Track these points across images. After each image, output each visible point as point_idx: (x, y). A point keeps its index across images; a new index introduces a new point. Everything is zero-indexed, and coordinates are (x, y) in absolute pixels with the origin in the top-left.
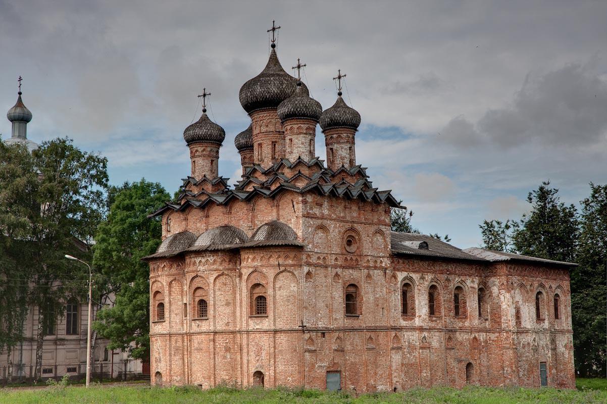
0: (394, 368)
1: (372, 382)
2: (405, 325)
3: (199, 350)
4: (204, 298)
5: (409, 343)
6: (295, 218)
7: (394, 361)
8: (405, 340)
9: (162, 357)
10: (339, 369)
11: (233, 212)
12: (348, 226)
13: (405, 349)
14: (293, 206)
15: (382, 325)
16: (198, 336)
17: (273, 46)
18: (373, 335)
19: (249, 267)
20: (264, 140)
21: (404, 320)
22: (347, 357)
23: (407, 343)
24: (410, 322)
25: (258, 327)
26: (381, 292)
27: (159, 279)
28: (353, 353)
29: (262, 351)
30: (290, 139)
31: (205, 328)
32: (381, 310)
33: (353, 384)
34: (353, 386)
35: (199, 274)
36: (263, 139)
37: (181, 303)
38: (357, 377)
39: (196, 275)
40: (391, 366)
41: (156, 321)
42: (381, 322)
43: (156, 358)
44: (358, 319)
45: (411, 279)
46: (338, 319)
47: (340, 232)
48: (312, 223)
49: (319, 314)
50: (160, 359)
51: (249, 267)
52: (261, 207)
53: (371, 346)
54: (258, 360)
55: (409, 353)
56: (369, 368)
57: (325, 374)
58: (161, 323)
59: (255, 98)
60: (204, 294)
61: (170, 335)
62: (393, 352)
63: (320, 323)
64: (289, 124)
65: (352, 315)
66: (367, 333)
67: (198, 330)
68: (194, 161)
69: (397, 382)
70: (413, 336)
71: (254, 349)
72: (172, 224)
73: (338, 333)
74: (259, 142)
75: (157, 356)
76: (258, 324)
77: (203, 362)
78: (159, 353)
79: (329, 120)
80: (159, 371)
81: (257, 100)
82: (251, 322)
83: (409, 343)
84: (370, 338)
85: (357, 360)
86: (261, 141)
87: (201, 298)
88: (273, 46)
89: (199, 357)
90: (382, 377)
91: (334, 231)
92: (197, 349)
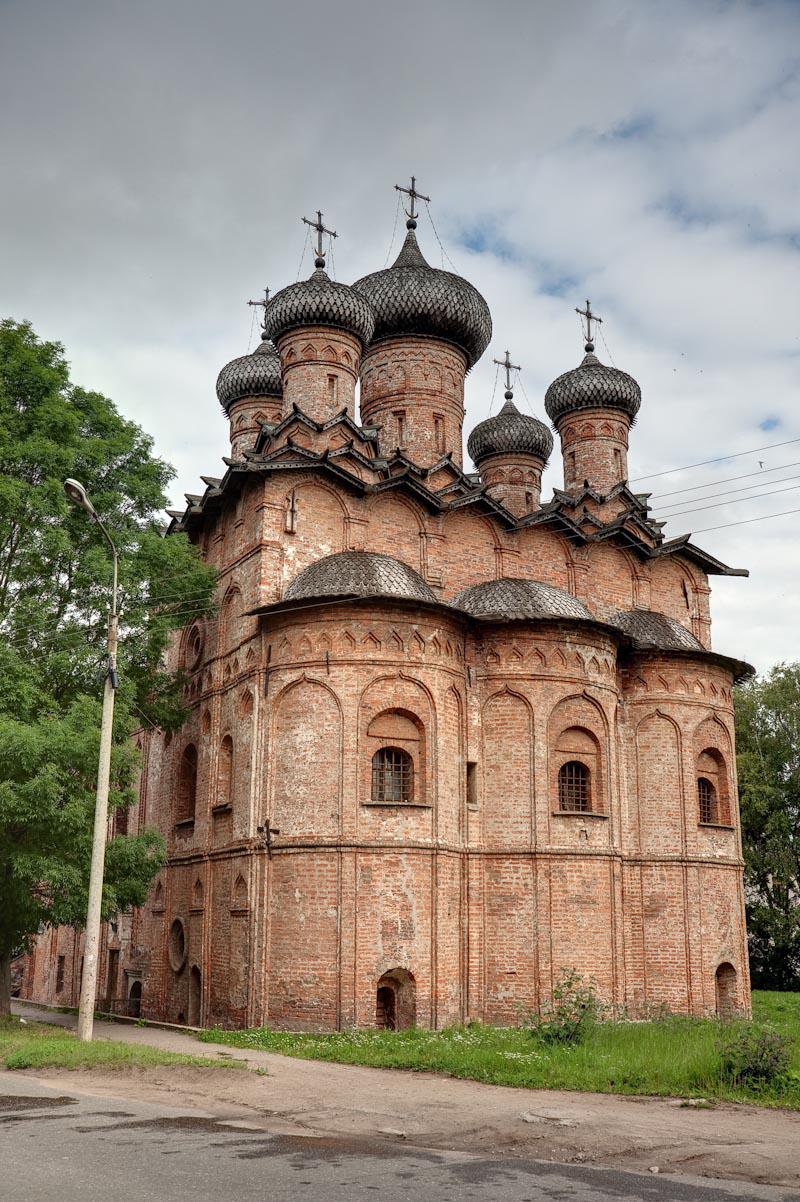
3: (584, 902)
4: (589, 761)
6: (690, 621)
9: (416, 920)
11: (524, 554)
14: (685, 595)
16: (583, 864)
17: (411, 225)
19: (700, 705)
20: (449, 411)
25: (720, 853)
27: (420, 674)
29: (731, 913)
30: (615, 449)
31: (600, 843)
35: (591, 691)
36: (448, 408)
37: (458, 759)
39: (580, 691)
41: (368, 800)
43: (385, 923)
50: (408, 932)
51: (700, 705)
52: (604, 569)
54: (724, 936)
58: (416, 811)
59: (464, 316)
60: (586, 749)
61: (435, 851)
64: (618, 418)
67: (581, 845)
68: (332, 378)
71: (716, 907)
72: (301, 516)
74: (436, 411)
75: (395, 916)
76: (721, 846)
77: (597, 937)
78: (406, 908)
79: (541, 437)
80: (403, 964)
81: (467, 321)
82: (705, 839)
86: (444, 413)
87: (574, 757)
88: (411, 225)
89: (585, 923)
92: (579, 900)
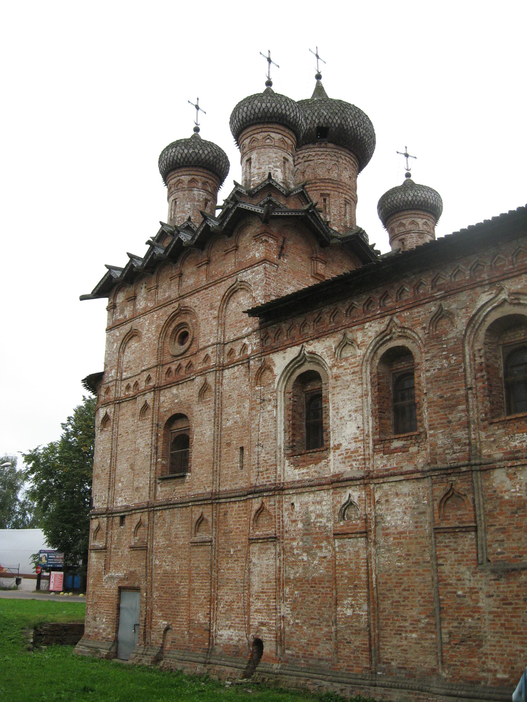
0: (256, 588)
1: (201, 617)
2: (297, 478)
5: (307, 522)
7: (256, 570)
8: (293, 518)
10: (136, 584)
12: (170, 310)
13: (294, 539)
15: (237, 486)
18: (207, 512)
21: (296, 465)
22: (157, 562)
23: (300, 525)
24: (313, 468)
26: (238, 413)
28: (169, 553)
32: (237, 453)
33: (165, 617)
34: (166, 623)
38: (174, 603)
40: (248, 585)
42: (235, 481)
44: (183, 482)
45: (314, 358)
46: (140, 488)
47: (157, 327)
48: (118, 334)
49: (120, 484)
53: (203, 536)
55: (308, 550)
56: (196, 584)
57: (116, 592)
62: (255, 548)
63: (120, 499)
65: (177, 475)
66: (195, 509)
69: (262, 624)
70: (320, 503)
73: (139, 515)
83: (307, 522)
84: (201, 520)
85: (176, 569)
90: (232, 610)
91: (148, 330)
